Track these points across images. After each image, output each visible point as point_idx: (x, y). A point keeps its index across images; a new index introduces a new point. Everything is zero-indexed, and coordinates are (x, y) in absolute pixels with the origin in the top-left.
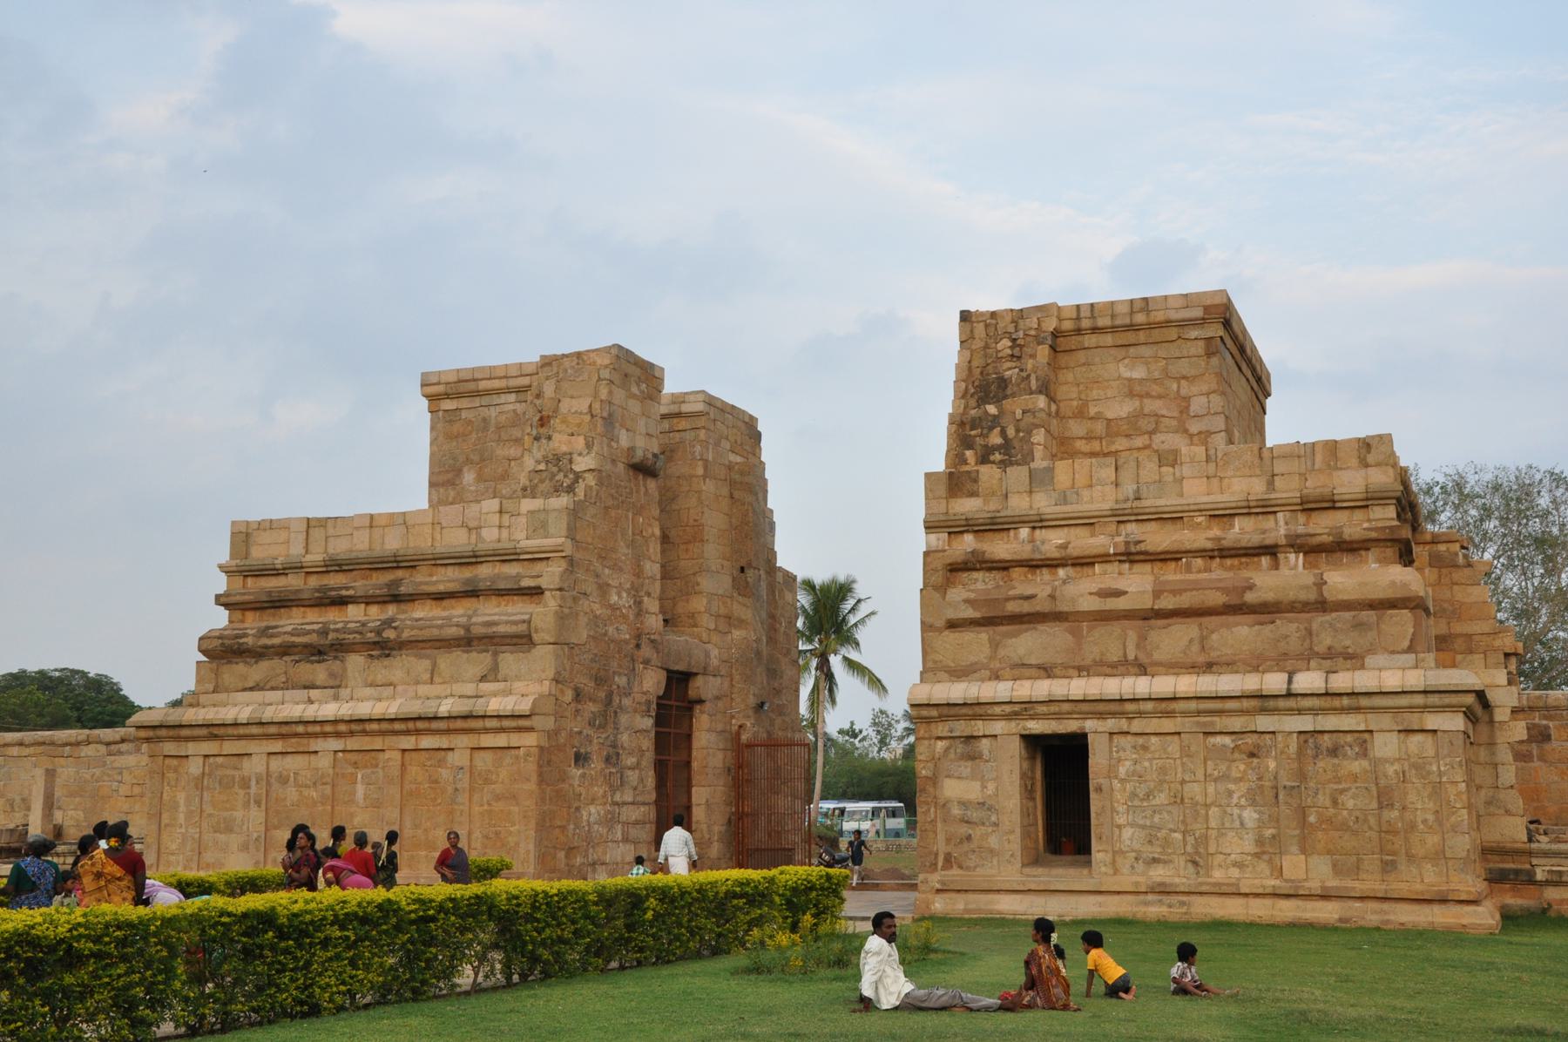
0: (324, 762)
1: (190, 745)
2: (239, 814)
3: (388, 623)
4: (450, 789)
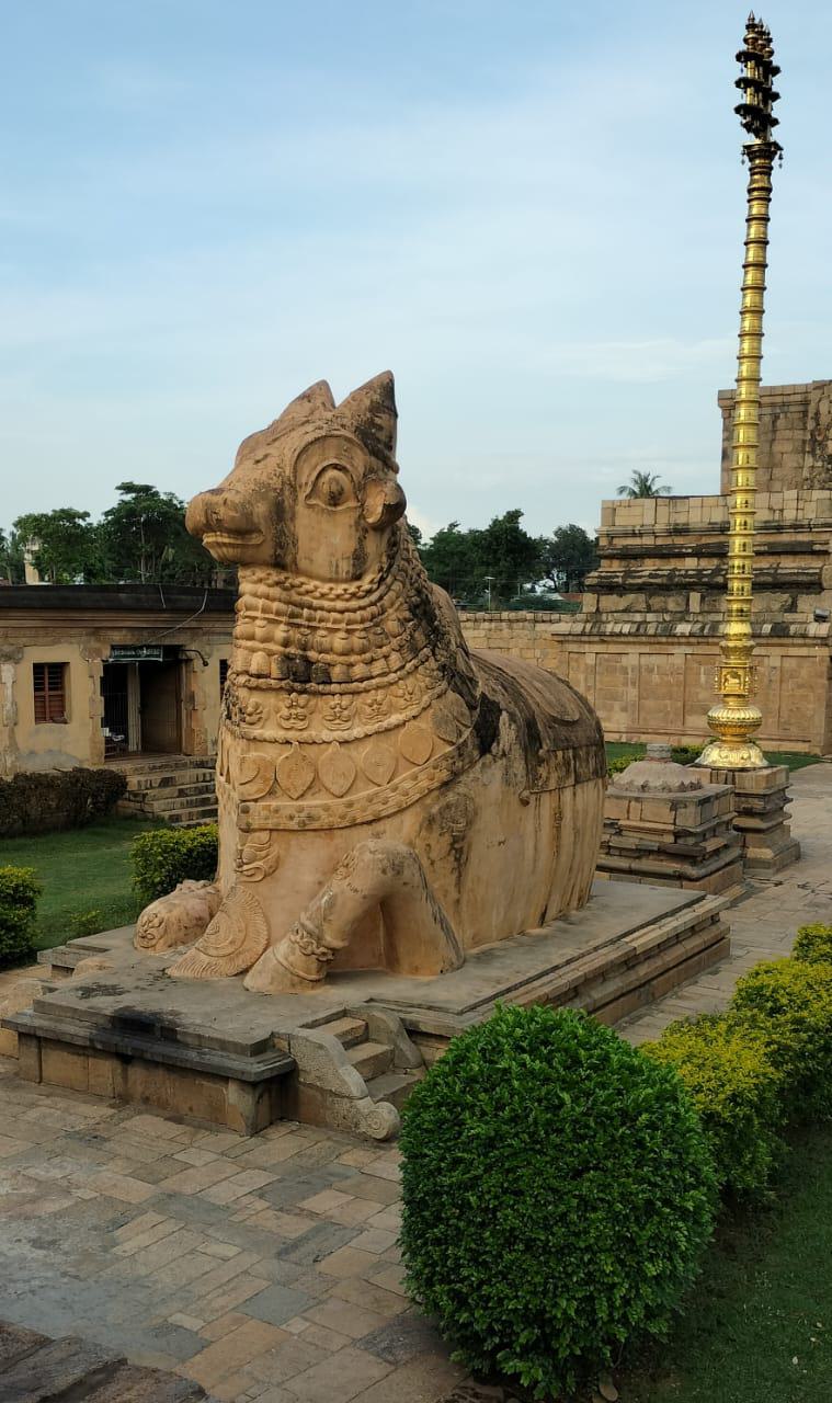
0: (678, 661)
1: (587, 646)
2: (620, 689)
3: (717, 571)
4: (766, 680)
